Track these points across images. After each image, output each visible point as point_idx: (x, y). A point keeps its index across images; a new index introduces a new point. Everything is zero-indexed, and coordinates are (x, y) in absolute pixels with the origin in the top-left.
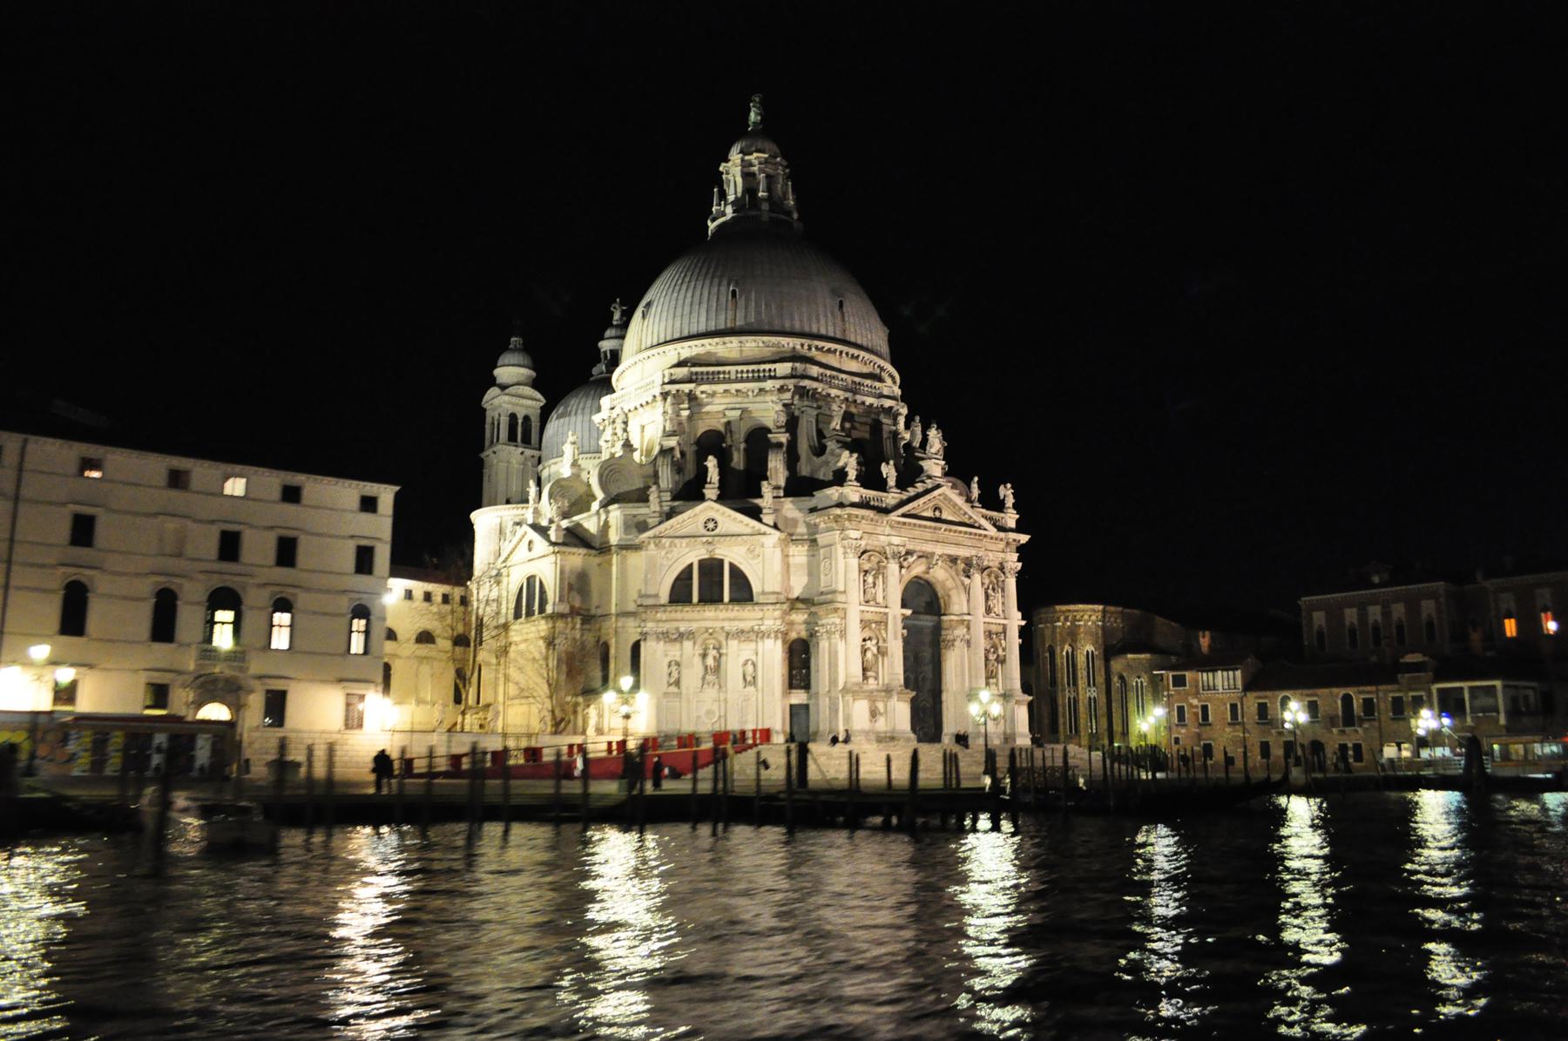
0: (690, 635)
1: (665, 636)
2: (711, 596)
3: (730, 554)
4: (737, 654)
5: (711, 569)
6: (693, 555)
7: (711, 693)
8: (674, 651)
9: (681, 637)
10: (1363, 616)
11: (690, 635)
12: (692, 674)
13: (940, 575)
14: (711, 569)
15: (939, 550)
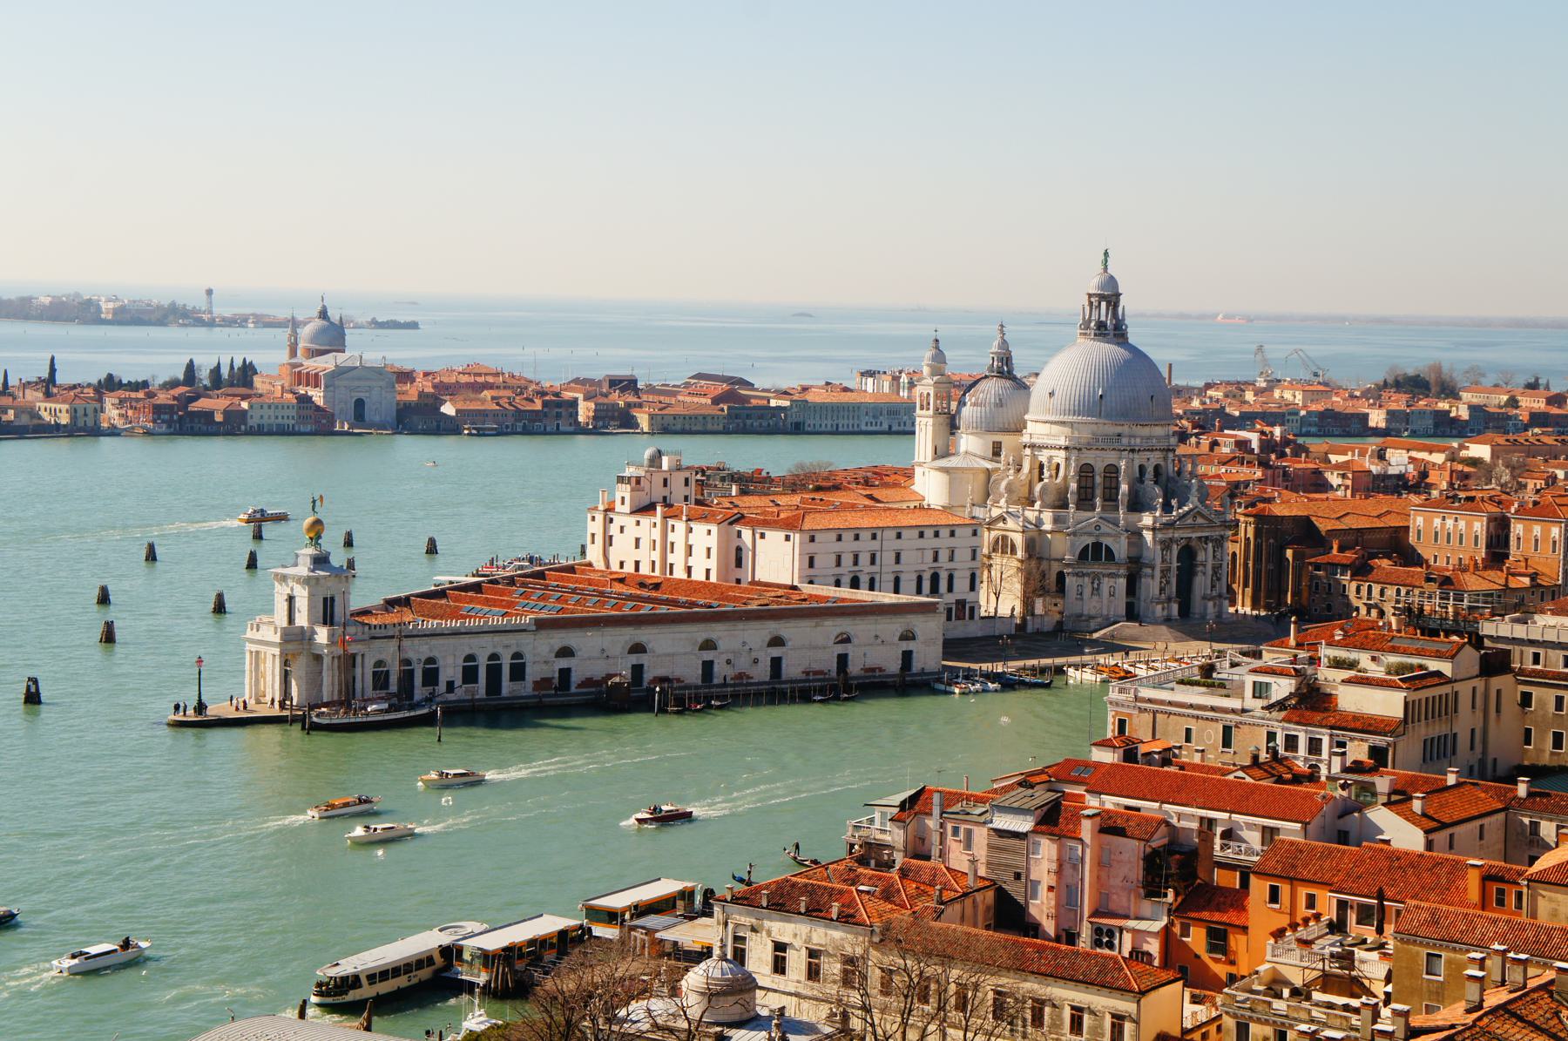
0: (1088, 575)
1: (1077, 575)
2: (1096, 557)
3: (1106, 541)
4: (1106, 583)
5: (1097, 546)
6: (1090, 540)
7: (1095, 598)
8: (1080, 581)
9: (1084, 575)
10: (1443, 525)
11: (1088, 575)
12: (1087, 591)
13: (1193, 544)
14: (1097, 546)
15: (1194, 535)
